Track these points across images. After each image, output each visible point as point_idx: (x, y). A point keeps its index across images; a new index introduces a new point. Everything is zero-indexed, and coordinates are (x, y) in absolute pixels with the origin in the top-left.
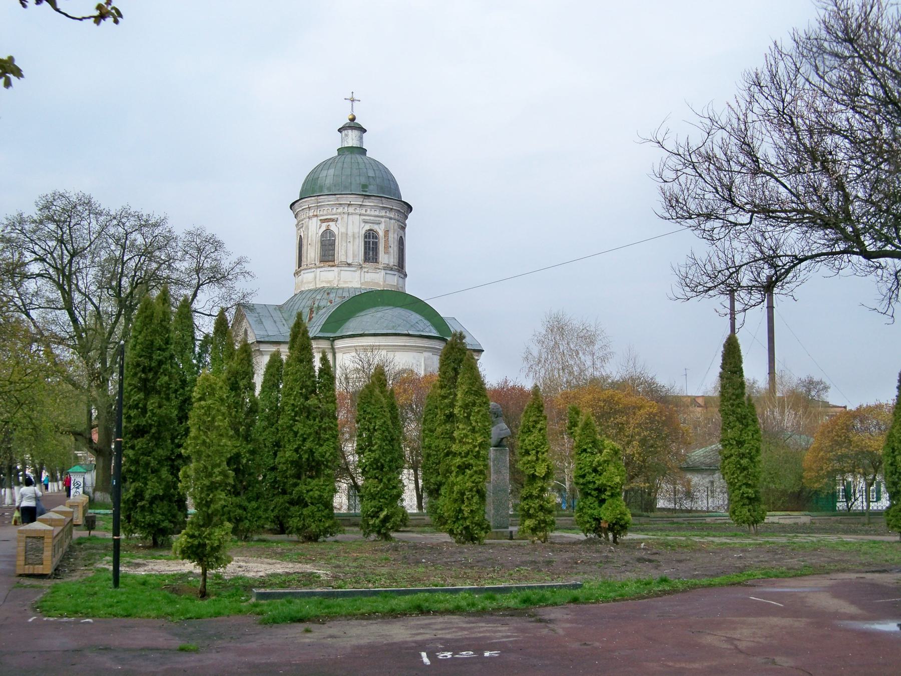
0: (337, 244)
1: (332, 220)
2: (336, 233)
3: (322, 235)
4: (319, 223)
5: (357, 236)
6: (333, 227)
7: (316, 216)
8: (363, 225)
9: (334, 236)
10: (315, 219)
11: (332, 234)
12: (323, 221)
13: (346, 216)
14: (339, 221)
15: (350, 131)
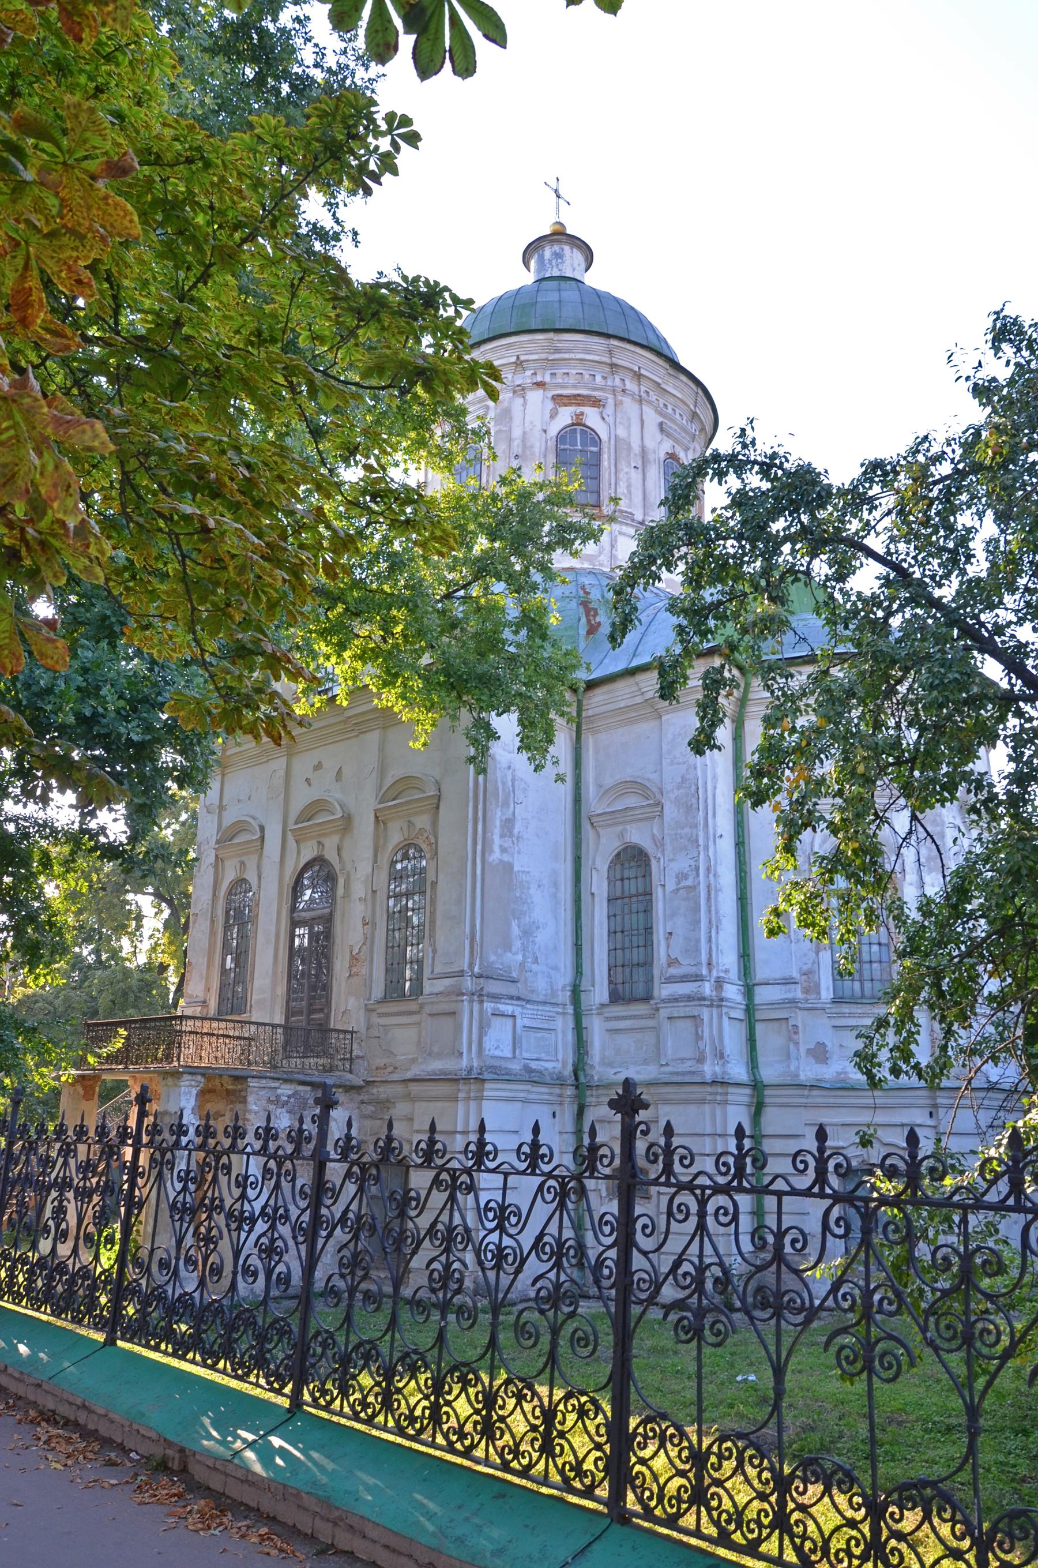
0: (605, 463)
1: (596, 403)
2: (604, 436)
3: (561, 438)
4: (550, 405)
5: (651, 457)
6: (592, 417)
7: (540, 385)
8: (658, 436)
9: (597, 440)
10: (535, 397)
11: (592, 437)
12: (560, 400)
13: (627, 401)
14: (609, 410)
15: (567, 248)
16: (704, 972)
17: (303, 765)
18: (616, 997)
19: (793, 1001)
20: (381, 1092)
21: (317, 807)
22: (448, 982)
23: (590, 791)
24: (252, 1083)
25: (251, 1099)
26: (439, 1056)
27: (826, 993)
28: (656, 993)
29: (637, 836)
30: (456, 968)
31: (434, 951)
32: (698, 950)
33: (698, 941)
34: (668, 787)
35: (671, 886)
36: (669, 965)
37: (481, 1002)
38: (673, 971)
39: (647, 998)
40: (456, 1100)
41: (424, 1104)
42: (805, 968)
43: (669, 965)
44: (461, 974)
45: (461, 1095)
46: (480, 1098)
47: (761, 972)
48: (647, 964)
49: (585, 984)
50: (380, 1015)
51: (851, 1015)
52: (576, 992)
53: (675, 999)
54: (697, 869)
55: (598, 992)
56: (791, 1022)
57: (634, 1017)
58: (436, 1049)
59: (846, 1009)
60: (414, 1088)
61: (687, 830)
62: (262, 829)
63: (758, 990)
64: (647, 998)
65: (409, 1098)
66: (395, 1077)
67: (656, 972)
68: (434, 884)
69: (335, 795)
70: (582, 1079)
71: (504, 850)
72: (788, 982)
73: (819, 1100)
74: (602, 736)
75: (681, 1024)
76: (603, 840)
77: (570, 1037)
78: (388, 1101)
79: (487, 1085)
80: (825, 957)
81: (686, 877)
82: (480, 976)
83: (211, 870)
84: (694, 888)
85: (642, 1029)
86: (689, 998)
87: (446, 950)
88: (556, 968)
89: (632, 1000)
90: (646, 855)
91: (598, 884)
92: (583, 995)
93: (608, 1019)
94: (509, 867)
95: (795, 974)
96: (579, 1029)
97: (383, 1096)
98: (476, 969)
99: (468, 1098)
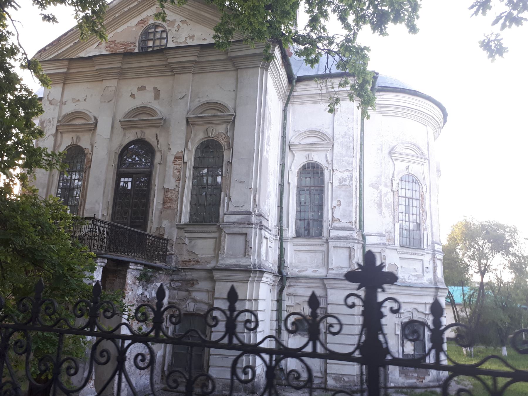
16: (354, 227)
17: (130, 86)
18: (298, 235)
19: (384, 244)
20: (189, 275)
21: (143, 110)
22: (239, 217)
23: (290, 133)
24: (132, 266)
25: (129, 276)
26: (233, 256)
27: (397, 243)
28: (325, 233)
29: (319, 158)
30: (244, 209)
31: (230, 199)
32: (351, 216)
33: (351, 211)
34: (336, 136)
35: (336, 183)
36: (333, 221)
37: (261, 229)
38: (336, 224)
39: (320, 236)
40: (247, 282)
41: (222, 283)
42: (388, 230)
43: (333, 221)
44: (249, 213)
45: (250, 279)
46: (259, 282)
47: (367, 229)
48: (320, 221)
49: (285, 228)
50: (186, 232)
51: (407, 253)
52: (281, 230)
53: (339, 238)
54: (351, 177)
55: (291, 231)
56: (382, 254)
57: (311, 245)
58: (231, 253)
59: (405, 250)
60: (216, 274)
61: (347, 158)
62: (96, 119)
63: (368, 238)
64: (320, 236)
65: (212, 280)
66: (197, 267)
67: (325, 225)
68: (230, 163)
69: (155, 105)
70: (285, 274)
71: (267, 152)
72: (381, 235)
73: (395, 291)
74: (296, 107)
75: (340, 251)
76: (296, 158)
77: (277, 252)
78: (193, 280)
79: (265, 275)
80: (397, 225)
81: (345, 180)
82: (261, 215)
83: (52, 139)
84: (350, 186)
85: (315, 251)
86: (346, 238)
87: (234, 200)
88: (272, 217)
89: (309, 236)
90: (321, 168)
91: (293, 179)
92: (284, 233)
93: (297, 245)
94: (267, 160)
95: (384, 233)
96: (282, 249)
97: (188, 277)
98: (256, 212)
99: (253, 282)
